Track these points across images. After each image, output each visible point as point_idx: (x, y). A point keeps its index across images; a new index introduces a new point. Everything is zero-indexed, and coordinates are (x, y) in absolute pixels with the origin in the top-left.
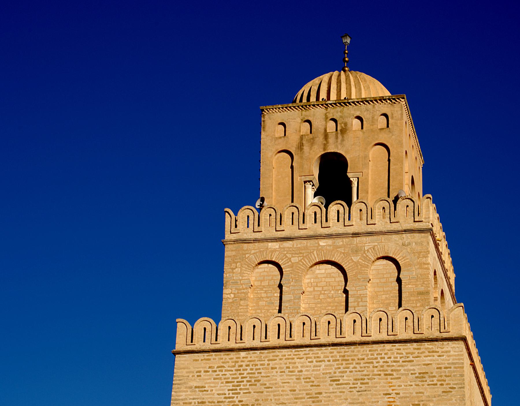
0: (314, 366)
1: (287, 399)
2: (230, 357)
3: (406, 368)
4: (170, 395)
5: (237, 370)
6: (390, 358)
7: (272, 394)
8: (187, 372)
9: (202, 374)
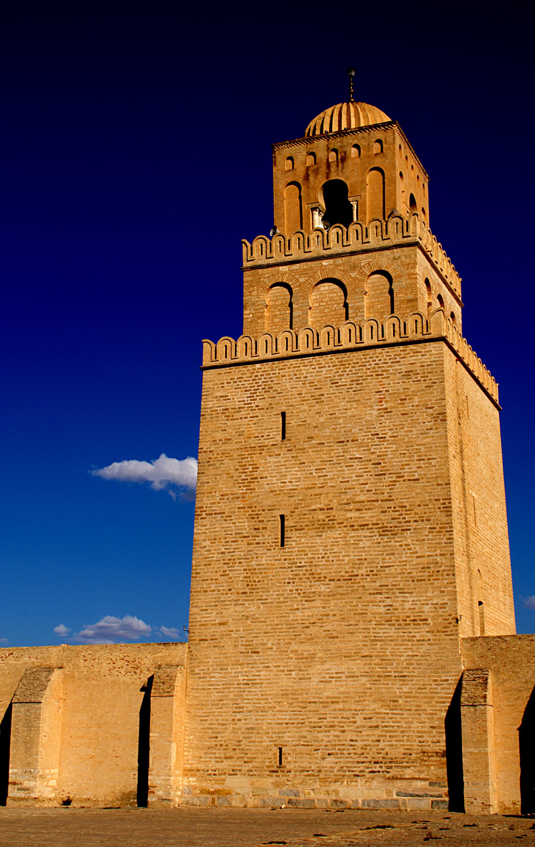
0: (317, 372)
1: (296, 402)
2: (248, 368)
3: (394, 368)
4: (200, 405)
5: (253, 380)
6: (380, 360)
7: (282, 398)
8: (213, 385)
9: (225, 385)
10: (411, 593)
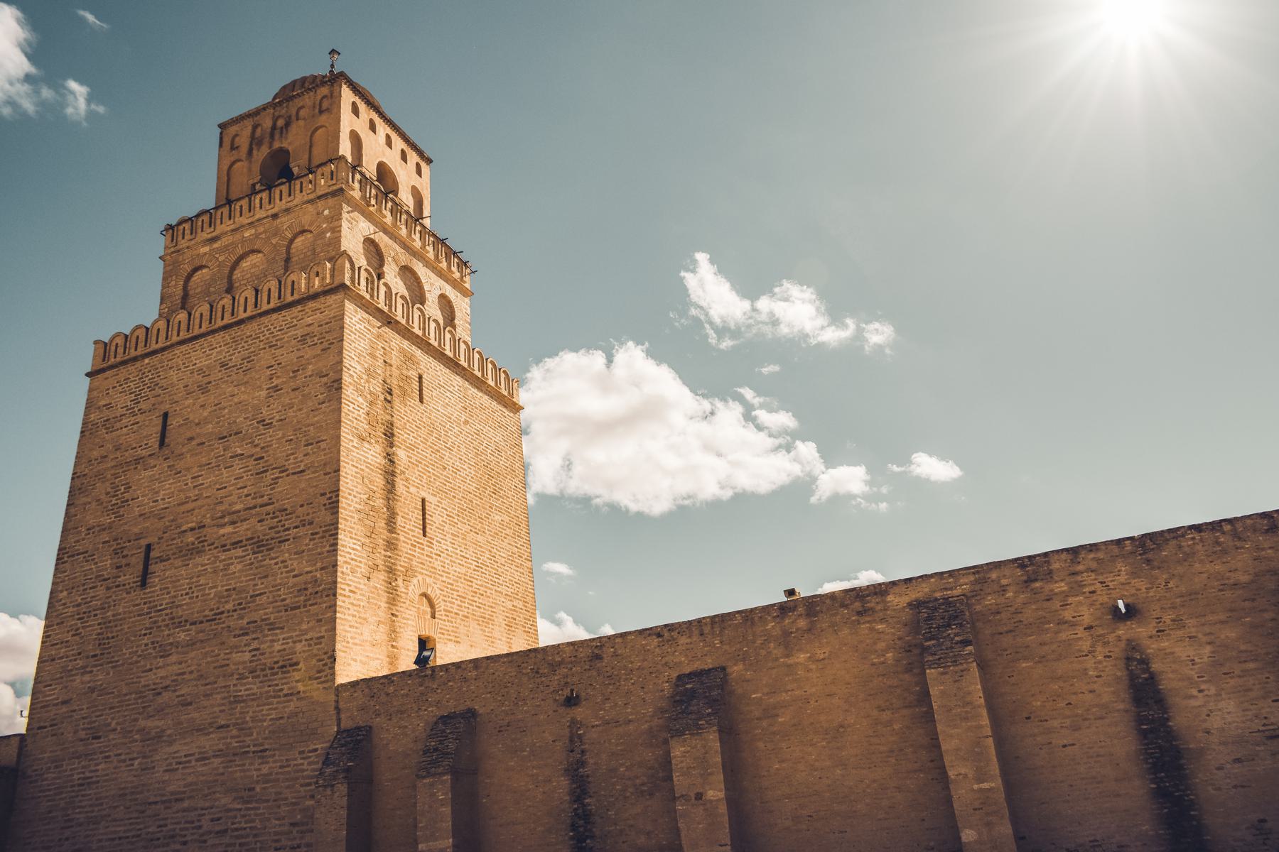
10: (282, 628)
